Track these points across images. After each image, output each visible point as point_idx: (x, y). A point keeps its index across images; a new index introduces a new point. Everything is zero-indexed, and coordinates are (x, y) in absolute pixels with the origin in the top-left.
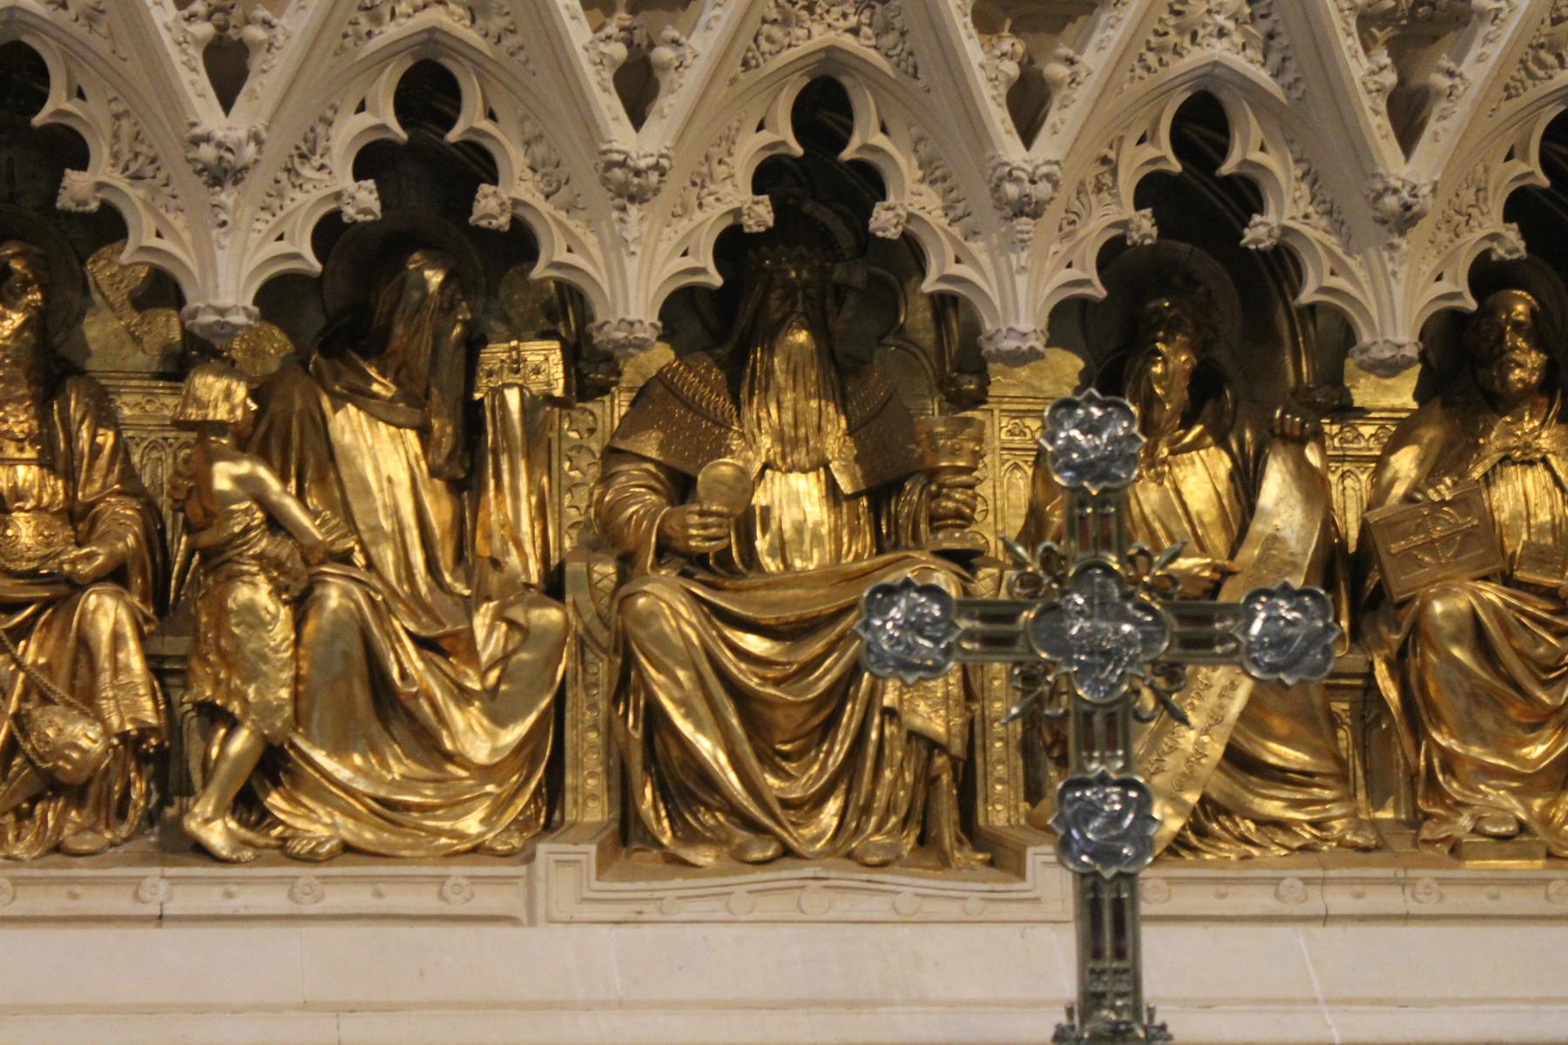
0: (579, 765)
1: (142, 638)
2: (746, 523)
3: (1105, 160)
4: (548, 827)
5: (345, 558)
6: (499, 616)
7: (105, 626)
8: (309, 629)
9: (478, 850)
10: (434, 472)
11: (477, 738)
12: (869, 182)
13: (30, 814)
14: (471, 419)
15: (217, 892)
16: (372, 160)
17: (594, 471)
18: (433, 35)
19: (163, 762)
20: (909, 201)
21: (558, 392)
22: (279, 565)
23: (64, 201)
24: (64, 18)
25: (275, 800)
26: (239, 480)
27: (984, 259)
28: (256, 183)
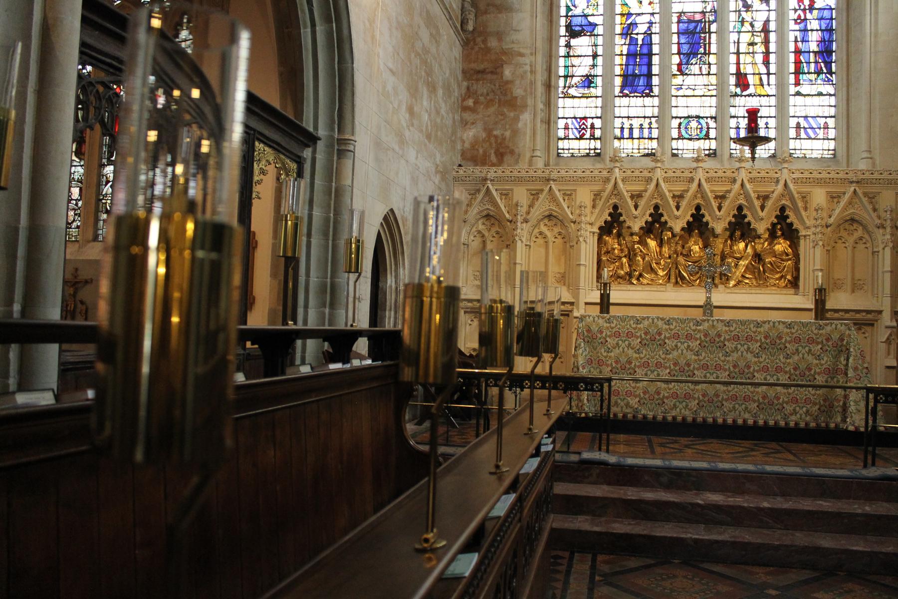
2: (690, 251)
11: (661, 273)
14: (662, 240)
16: (651, 215)
19: (630, 275)
20: (707, 218)
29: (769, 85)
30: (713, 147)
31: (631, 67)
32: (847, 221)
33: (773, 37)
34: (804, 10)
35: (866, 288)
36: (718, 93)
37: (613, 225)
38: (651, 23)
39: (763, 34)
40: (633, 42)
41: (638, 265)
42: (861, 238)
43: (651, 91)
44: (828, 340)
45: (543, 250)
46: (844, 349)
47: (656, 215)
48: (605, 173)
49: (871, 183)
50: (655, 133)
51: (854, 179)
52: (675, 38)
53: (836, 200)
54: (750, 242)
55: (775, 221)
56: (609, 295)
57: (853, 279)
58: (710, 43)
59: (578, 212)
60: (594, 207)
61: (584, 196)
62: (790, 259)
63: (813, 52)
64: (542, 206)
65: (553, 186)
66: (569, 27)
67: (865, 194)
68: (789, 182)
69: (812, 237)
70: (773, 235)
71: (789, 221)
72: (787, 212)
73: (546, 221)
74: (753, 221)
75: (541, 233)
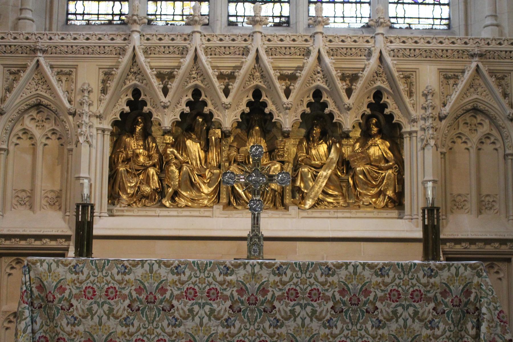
0: (222, 193)
1: (157, 174)
3: (301, 100)
4: (218, 202)
5: (188, 163)
6: (209, 171)
7: (151, 173)
8: (181, 173)
9: (206, 206)
10: (202, 149)
11: (206, 189)
12: (265, 105)
13: (141, 200)
15: (167, 212)
16: (188, 104)
17: (228, 149)
18: (196, 85)
19: (161, 192)
20: (271, 108)
21: (220, 137)
22: (176, 164)
23: (144, 111)
24: (143, 85)
25: (177, 199)
26: (171, 152)
27: (282, 116)
28: (171, 108)
30: (286, 13)
32: (468, 111)
35: (497, 206)
37: (134, 119)
41: (171, 179)
42: (488, 136)
44: (444, 294)
45: (28, 158)
46: (471, 308)
47: (197, 102)
48: (119, 40)
49: (499, 57)
51: (476, 51)
53: (451, 82)
54: (334, 143)
55: (368, 111)
56: (90, 225)
57: (479, 194)
59: (79, 98)
60: (104, 91)
61: (89, 75)
62: (390, 167)
64: (25, 90)
65: (42, 61)
67: (492, 73)
68: (385, 54)
69: (420, 133)
70: (366, 136)
71: (387, 111)
72: (384, 99)
73: (34, 113)
74: (336, 111)
75: (25, 132)
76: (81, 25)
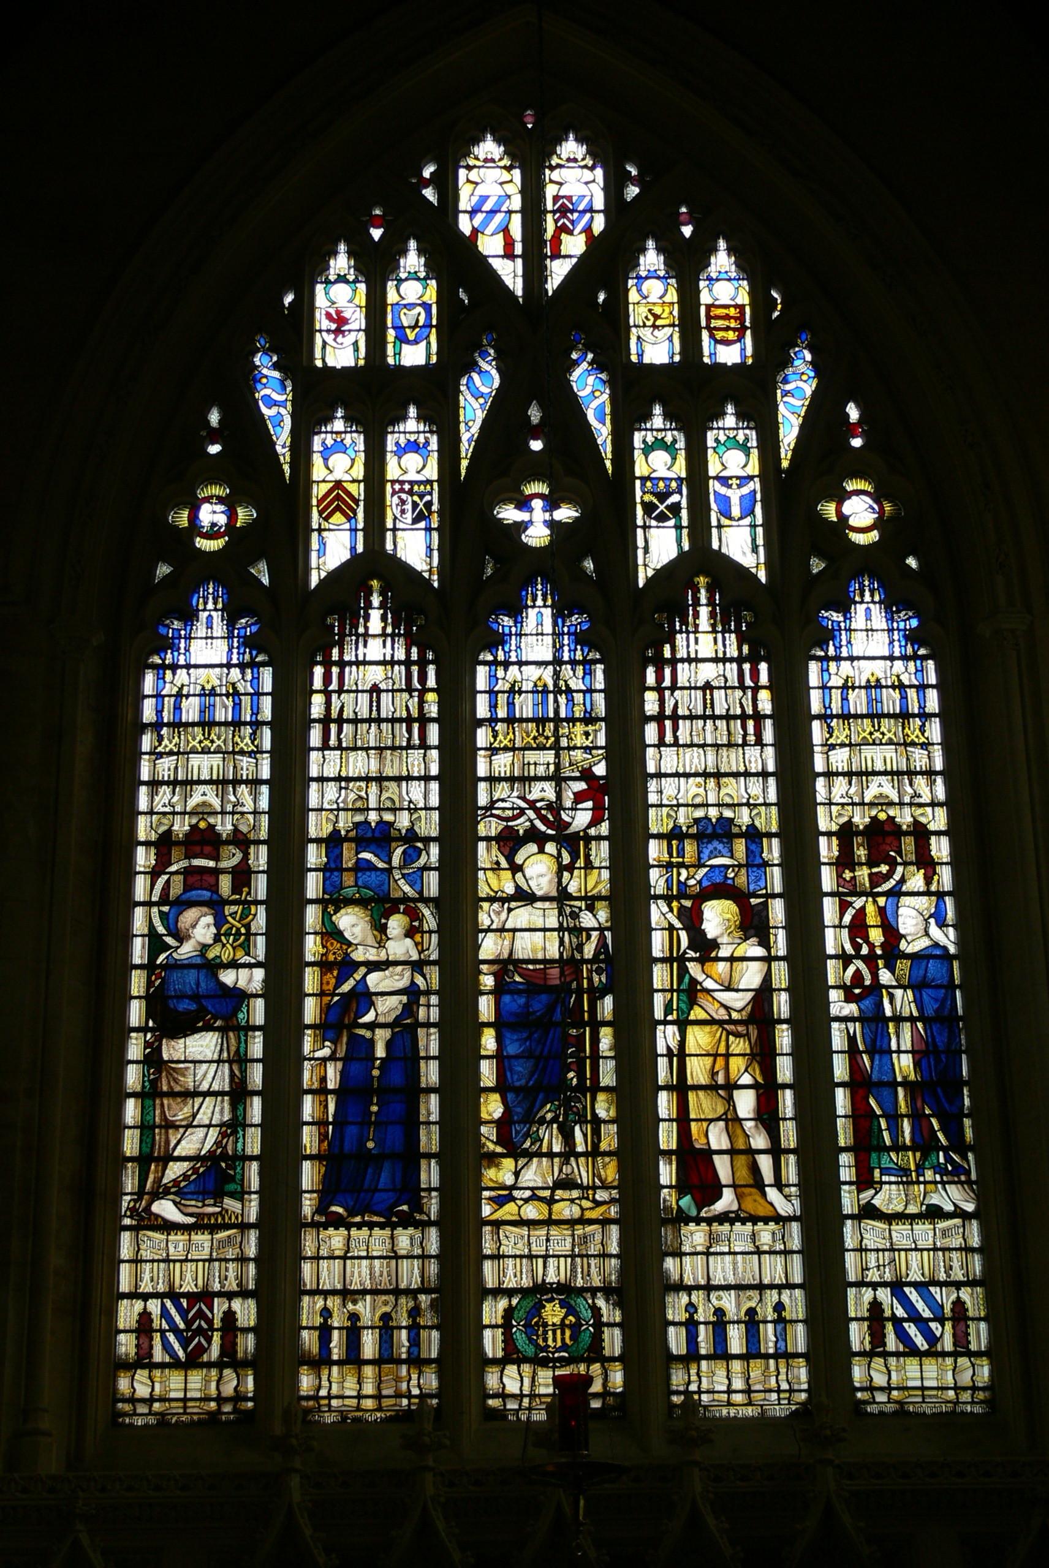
29: (779, 1185)
31: (352, 1131)
33: (784, 1038)
34: (870, 960)
36: (621, 1212)
38: (412, 993)
39: (754, 1032)
40: (360, 1050)
43: (417, 1206)
50: (432, 1343)
52: (489, 1041)
58: (596, 1056)
63: (905, 1083)
66: (154, 1001)
76: (146, 1426)
